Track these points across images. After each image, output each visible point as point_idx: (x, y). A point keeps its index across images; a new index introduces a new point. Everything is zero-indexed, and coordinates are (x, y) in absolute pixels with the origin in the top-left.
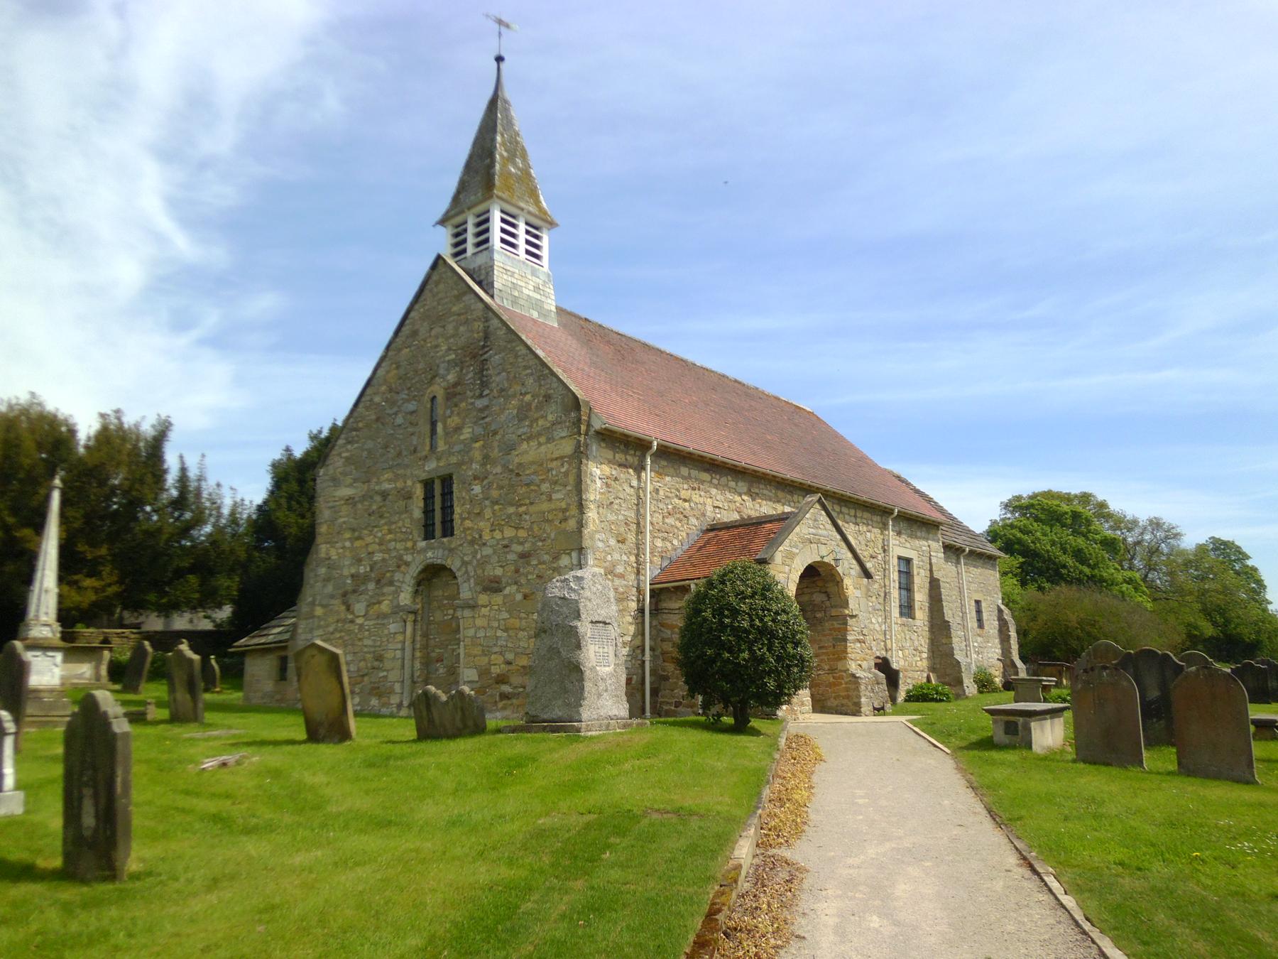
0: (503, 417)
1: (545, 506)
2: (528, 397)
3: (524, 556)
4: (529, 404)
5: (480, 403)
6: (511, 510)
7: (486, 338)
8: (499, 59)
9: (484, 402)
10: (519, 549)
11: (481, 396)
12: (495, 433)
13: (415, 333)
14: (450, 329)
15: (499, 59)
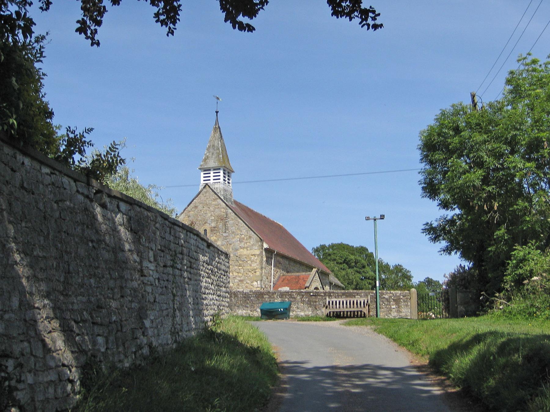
0: (233, 240)
1: (249, 267)
2: (243, 236)
3: (240, 281)
4: (244, 238)
5: (224, 235)
6: (236, 267)
7: (227, 215)
8: (217, 112)
9: (227, 234)
10: (239, 279)
11: (225, 232)
12: (230, 244)
13: (196, 207)
14: (212, 209)
15: (217, 112)
